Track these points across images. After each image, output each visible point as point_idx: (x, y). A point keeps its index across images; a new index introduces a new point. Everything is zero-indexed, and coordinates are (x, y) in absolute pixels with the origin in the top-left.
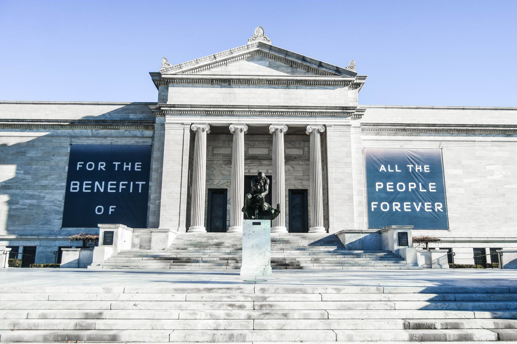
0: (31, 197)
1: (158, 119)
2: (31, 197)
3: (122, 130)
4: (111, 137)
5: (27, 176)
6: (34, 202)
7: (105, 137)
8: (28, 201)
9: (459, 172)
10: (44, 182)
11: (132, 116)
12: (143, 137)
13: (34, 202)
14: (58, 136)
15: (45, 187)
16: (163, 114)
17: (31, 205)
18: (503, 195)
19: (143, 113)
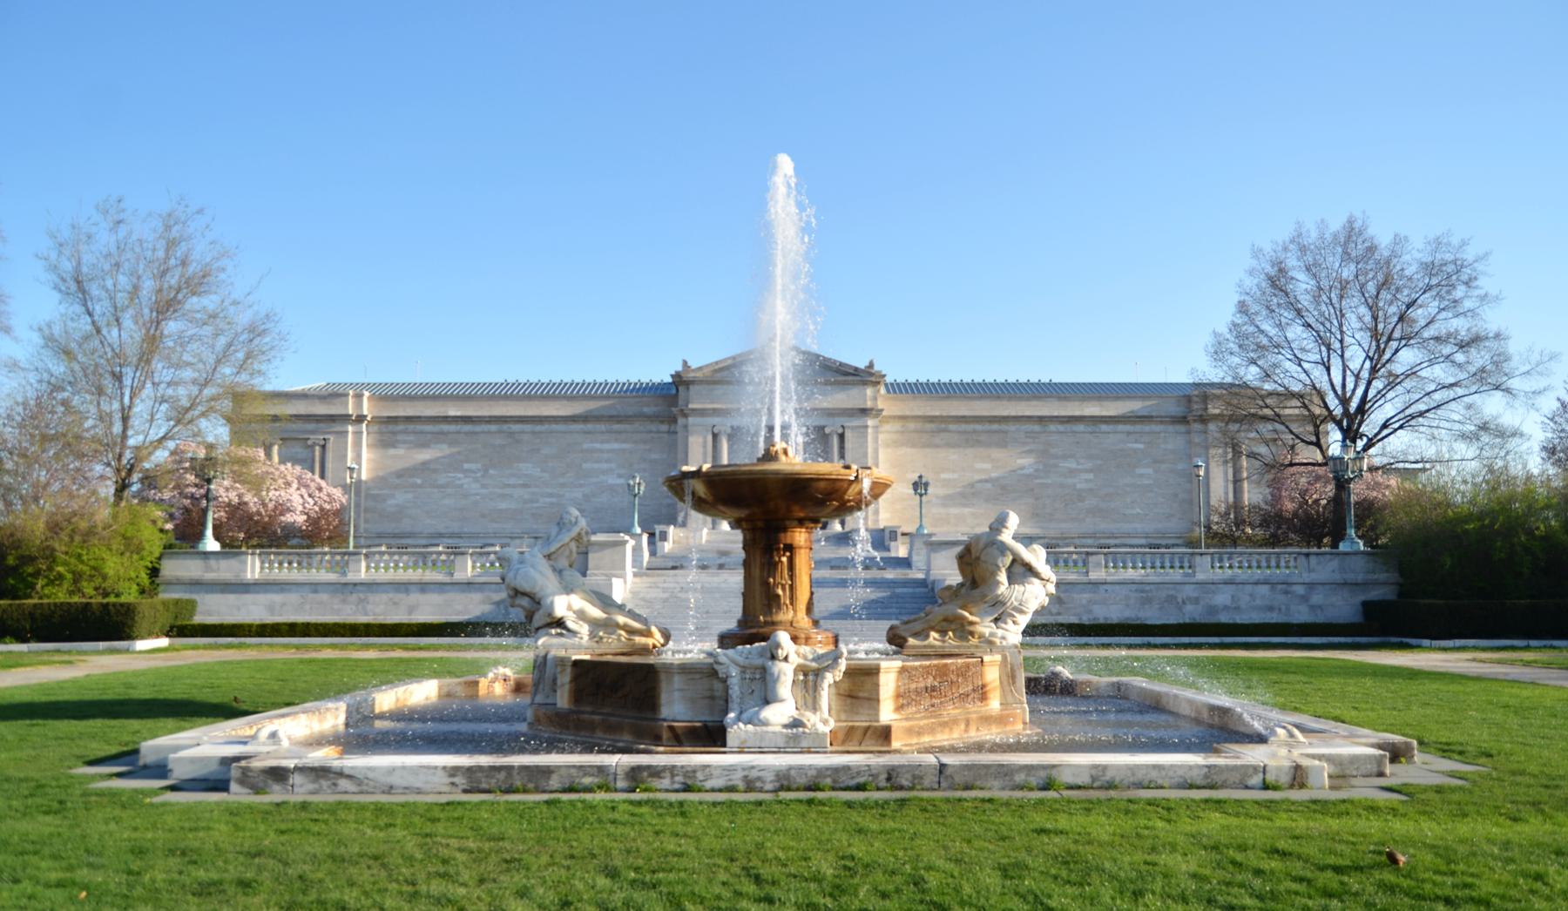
0: (551, 495)
1: (681, 421)
2: (551, 495)
3: (637, 426)
4: (626, 432)
5: (546, 475)
6: (554, 500)
7: (620, 432)
8: (548, 500)
9: (987, 466)
10: (562, 480)
11: (646, 410)
12: (658, 432)
13: (554, 500)
14: (571, 432)
15: (563, 485)
16: (686, 416)
17: (552, 504)
18: (1032, 490)
19: (656, 406)
